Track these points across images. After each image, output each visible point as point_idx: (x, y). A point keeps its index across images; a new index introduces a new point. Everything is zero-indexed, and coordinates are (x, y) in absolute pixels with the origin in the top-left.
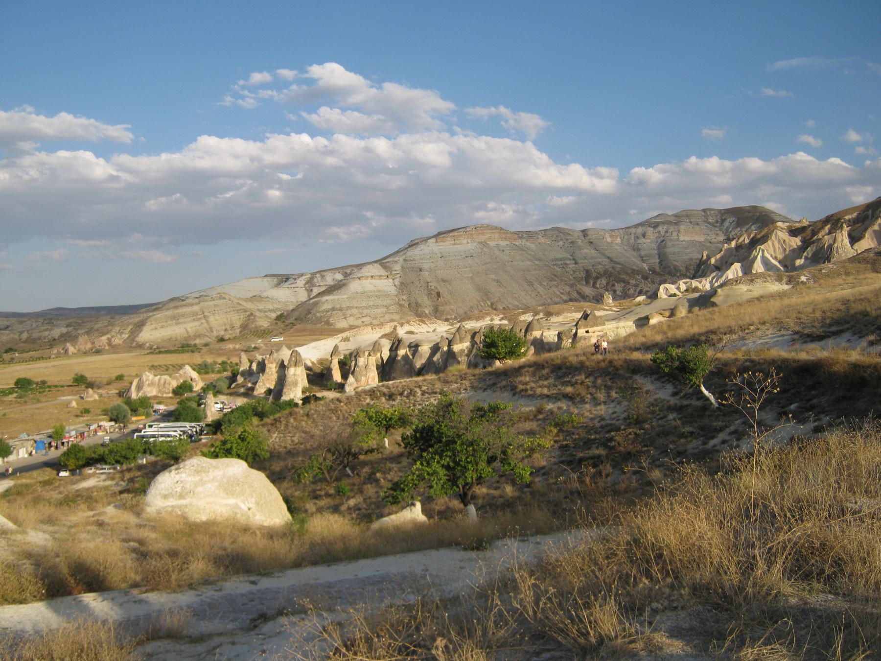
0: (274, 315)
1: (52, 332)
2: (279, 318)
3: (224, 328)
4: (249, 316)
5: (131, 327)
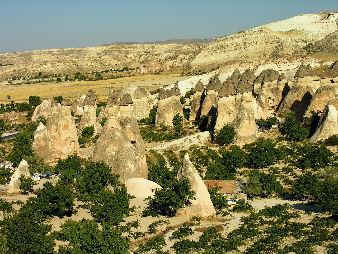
0: (304, 45)
1: (160, 56)
2: (306, 48)
3: (259, 55)
4: (279, 46)
5: (191, 54)
